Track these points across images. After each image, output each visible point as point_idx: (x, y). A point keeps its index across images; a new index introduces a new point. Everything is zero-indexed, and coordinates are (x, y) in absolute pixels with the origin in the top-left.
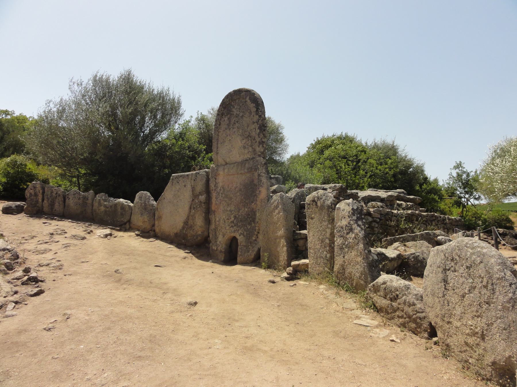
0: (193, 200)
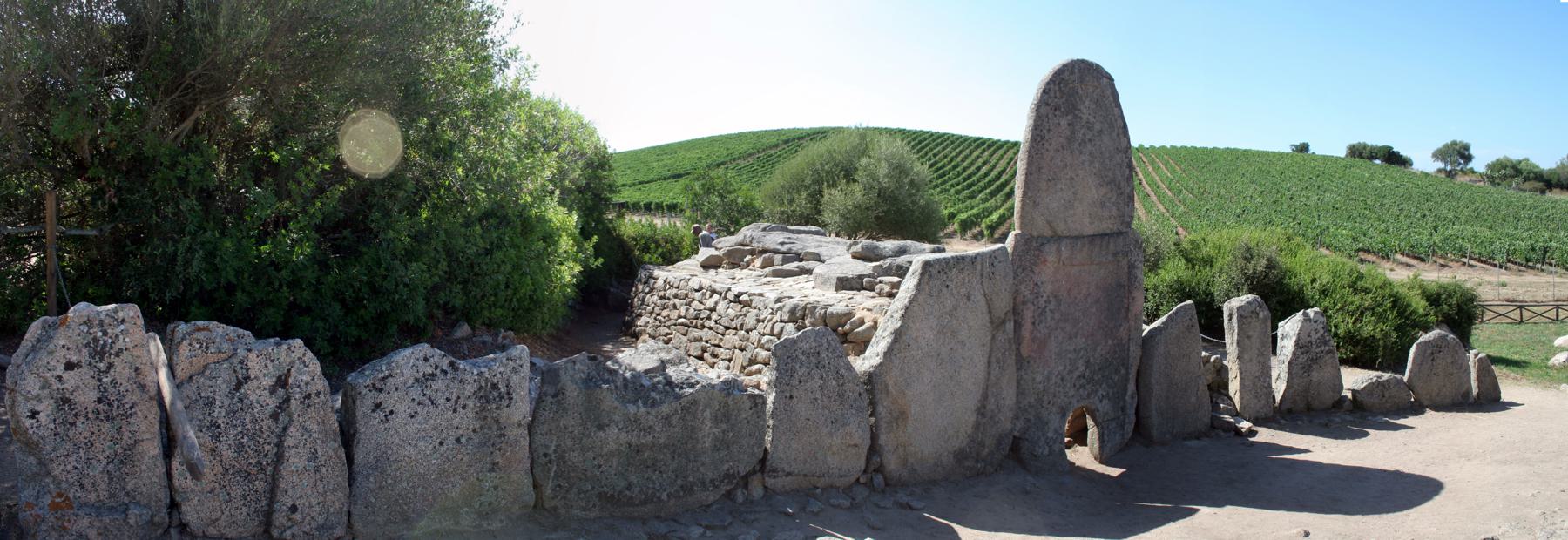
0: (993, 337)
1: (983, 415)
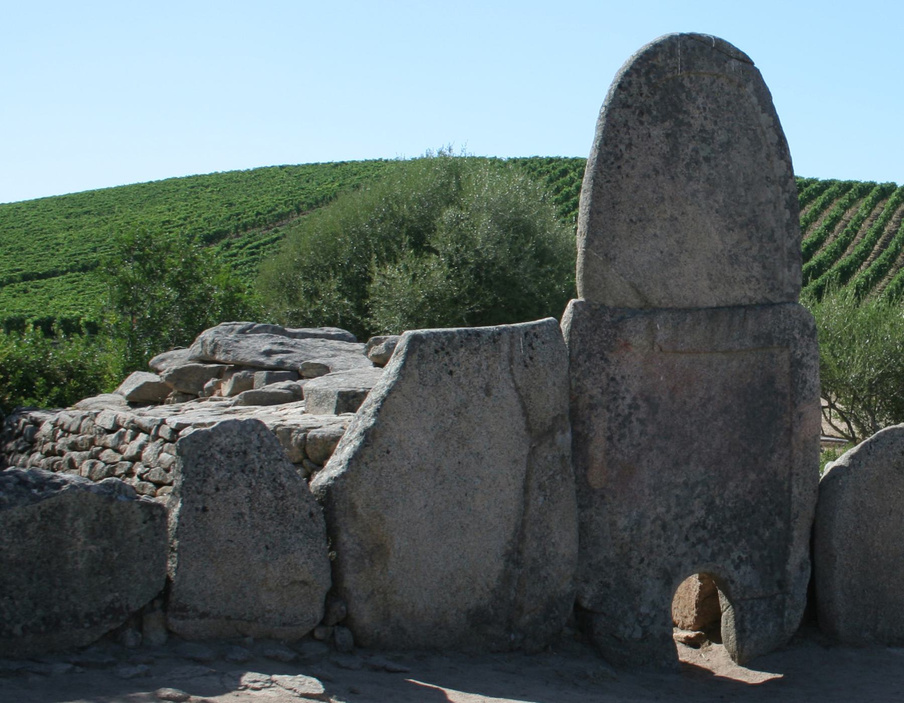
0: (533, 452)
1: (517, 564)
